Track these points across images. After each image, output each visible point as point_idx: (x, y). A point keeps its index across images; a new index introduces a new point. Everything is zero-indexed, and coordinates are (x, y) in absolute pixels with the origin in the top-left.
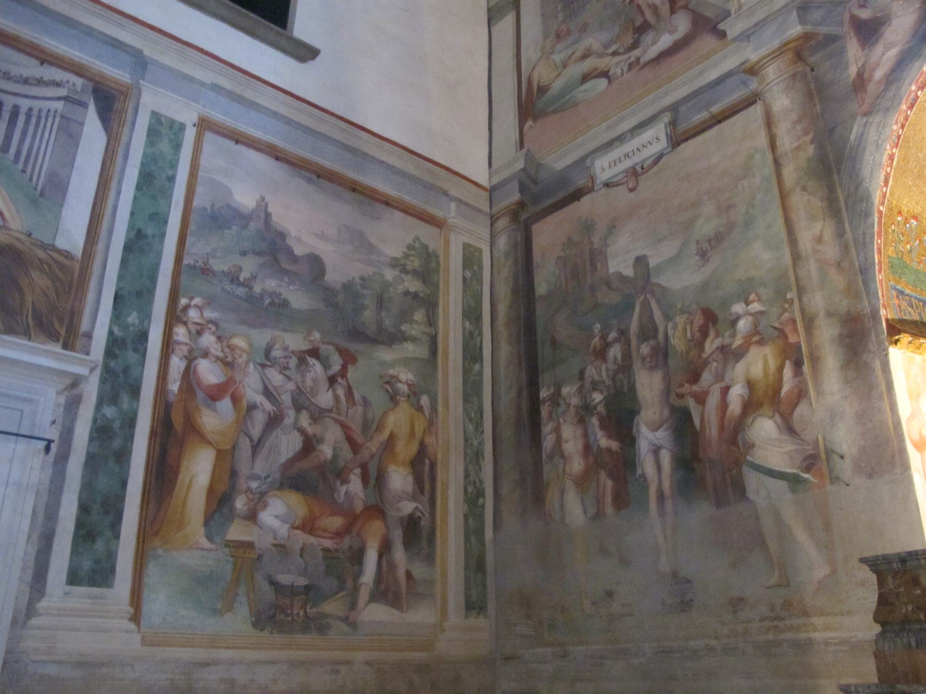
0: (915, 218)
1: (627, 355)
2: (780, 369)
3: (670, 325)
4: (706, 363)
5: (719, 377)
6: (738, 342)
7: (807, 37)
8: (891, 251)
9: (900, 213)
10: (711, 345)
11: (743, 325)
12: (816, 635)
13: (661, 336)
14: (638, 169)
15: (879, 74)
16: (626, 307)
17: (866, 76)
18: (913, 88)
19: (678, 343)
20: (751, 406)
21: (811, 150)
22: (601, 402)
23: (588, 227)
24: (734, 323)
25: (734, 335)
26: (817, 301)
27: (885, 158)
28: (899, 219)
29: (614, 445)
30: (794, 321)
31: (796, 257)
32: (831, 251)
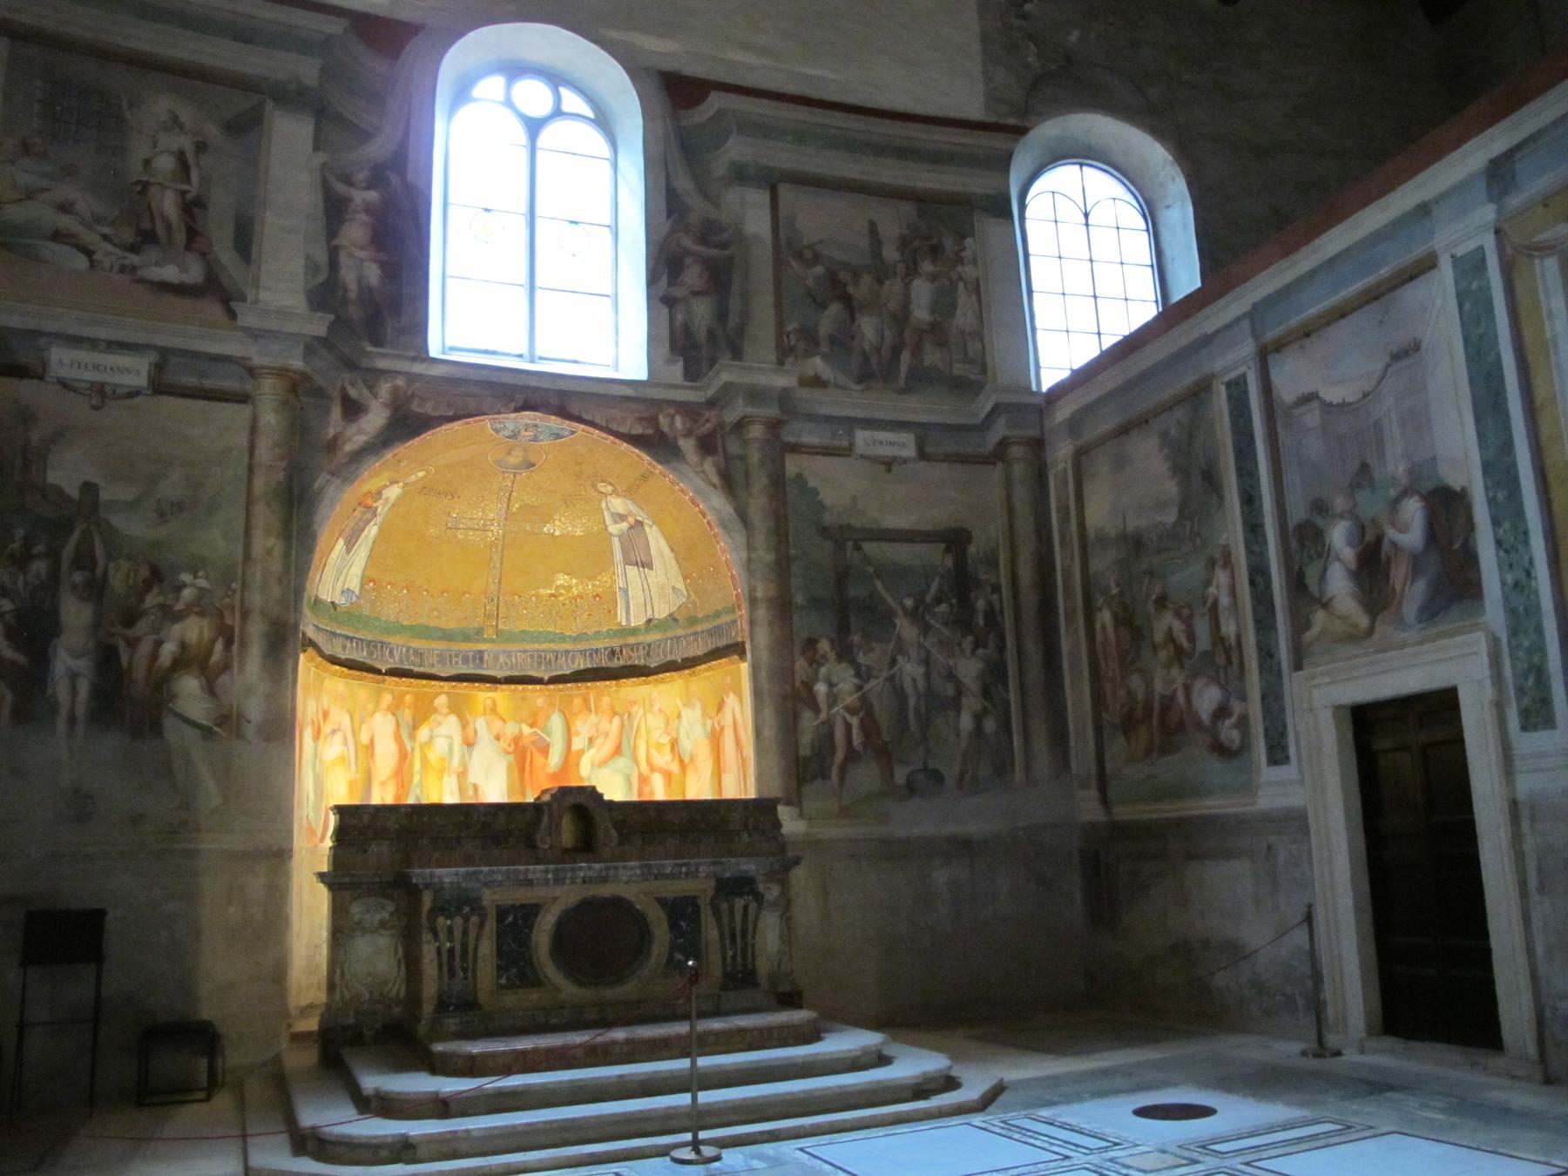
1: (54, 576)
2: (213, 642)
3: (112, 565)
4: (144, 613)
5: (156, 630)
6: (179, 607)
7: (305, 377)
10: (151, 600)
11: (187, 593)
12: (201, 846)
13: (99, 571)
14: (108, 389)
15: (349, 448)
16: (61, 528)
17: (339, 442)
19: (117, 582)
20: (182, 662)
21: (281, 476)
22: (11, 611)
23: (27, 417)
24: (179, 588)
25: (177, 599)
26: (256, 599)
29: (21, 659)
30: (233, 609)
31: (247, 556)
32: (276, 566)
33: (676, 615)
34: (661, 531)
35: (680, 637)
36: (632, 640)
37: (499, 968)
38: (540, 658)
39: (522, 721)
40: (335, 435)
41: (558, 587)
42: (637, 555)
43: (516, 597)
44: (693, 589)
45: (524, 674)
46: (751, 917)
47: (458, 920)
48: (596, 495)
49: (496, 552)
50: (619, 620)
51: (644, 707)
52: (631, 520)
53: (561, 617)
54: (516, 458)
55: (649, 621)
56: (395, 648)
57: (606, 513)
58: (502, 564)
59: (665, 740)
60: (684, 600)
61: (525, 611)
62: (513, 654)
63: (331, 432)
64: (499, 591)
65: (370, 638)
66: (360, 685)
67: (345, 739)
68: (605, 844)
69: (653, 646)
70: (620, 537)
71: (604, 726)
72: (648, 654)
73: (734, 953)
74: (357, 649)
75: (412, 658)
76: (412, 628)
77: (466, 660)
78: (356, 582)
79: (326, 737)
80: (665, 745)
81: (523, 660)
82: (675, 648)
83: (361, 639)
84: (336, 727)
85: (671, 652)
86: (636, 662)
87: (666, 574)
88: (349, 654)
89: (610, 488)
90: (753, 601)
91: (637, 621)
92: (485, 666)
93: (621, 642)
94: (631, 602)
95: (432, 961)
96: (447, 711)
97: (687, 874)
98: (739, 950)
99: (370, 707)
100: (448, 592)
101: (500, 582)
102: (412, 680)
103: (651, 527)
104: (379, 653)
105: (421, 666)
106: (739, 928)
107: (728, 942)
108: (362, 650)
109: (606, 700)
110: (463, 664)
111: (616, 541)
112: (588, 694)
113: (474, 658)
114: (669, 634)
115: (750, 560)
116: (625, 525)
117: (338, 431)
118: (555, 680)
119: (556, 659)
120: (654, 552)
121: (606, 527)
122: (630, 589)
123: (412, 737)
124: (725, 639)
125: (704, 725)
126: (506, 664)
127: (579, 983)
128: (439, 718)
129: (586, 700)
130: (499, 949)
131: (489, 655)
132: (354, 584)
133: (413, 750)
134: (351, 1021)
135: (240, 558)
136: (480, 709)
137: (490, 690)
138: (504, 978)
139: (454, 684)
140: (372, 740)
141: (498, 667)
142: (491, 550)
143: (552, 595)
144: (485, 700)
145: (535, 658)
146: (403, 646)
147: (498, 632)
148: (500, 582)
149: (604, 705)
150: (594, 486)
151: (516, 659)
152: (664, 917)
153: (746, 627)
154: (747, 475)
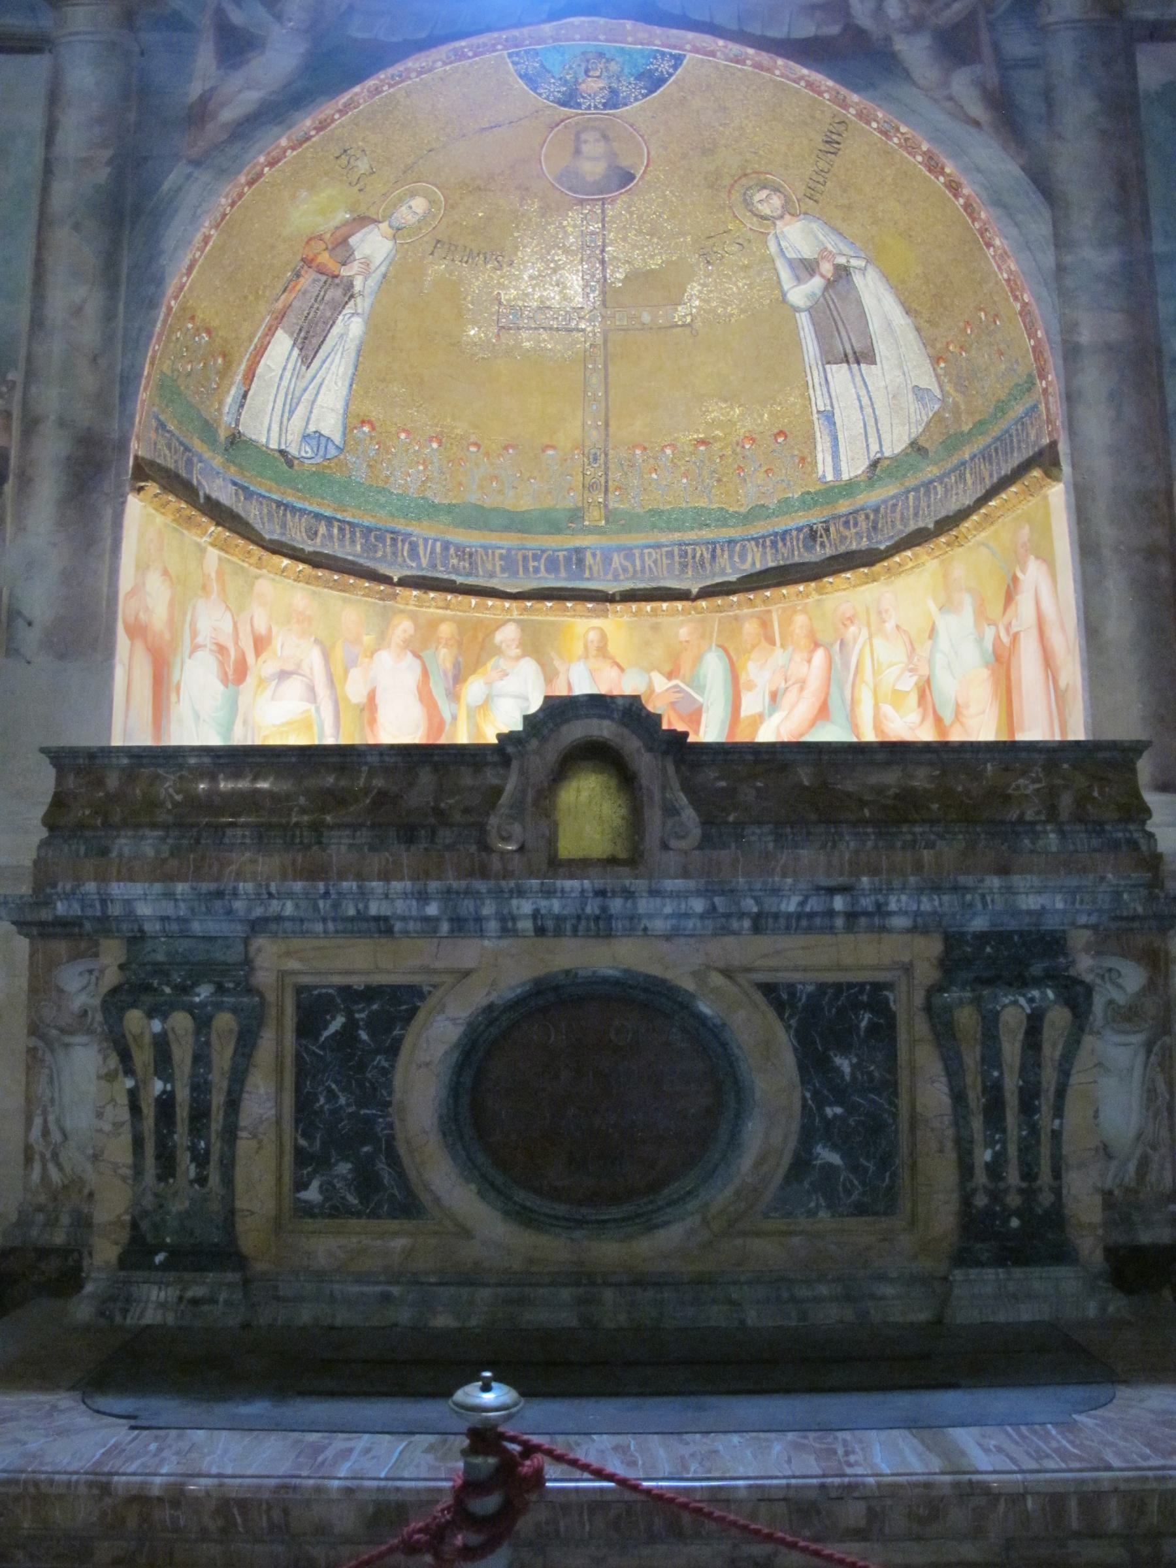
0: (208, 332)
8: (166, 367)
9: (192, 318)
15: (228, 115)
17: (211, 106)
18: (262, 159)
21: (102, 175)
27: (199, 237)
28: (190, 326)
31: (37, 323)
32: (89, 335)
33: (922, 442)
34: (886, 277)
35: (931, 482)
36: (844, 507)
37: (302, 1157)
38: (684, 556)
39: (652, 668)
40: (201, 96)
41: (712, 425)
42: (845, 339)
43: (638, 452)
44: (950, 381)
45: (654, 585)
46: (1052, 1051)
47: (181, 1021)
48: (752, 223)
49: (595, 370)
50: (820, 473)
51: (869, 625)
52: (827, 268)
53: (719, 480)
54: (593, 168)
55: (875, 464)
56: (421, 542)
57: (781, 265)
58: (606, 392)
59: (909, 683)
60: (937, 407)
61: (654, 476)
62: (637, 552)
63: (195, 90)
64: (606, 440)
65: (367, 521)
66: (344, 600)
67: (312, 689)
68: (665, 846)
69: (882, 510)
70: (809, 310)
71: (799, 668)
72: (875, 528)
73: (996, 1156)
74: (342, 540)
75: (455, 561)
76: (450, 509)
77: (553, 566)
78: (333, 421)
79: (262, 682)
80: (908, 692)
81: (655, 562)
82: (923, 504)
83: (349, 523)
84: (289, 667)
85: (916, 514)
86: (854, 547)
87: (901, 367)
88: (323, 545)
89: (777, 201)
90: (1071, 353)
91: (853, 467)
92: (587, 575)
93: (826, 513)
94: (840, 436)
95: (117, 1125)
96: (518, 651)
97: (852, 916)
98: (1012, 1150)
99: (368, 639)
100: (513, 447)
101: (607, 425)
102: (449, 597)
103: (863, 271)
104: (388, 549)
105: (469, 575)
106: (1011, 1084)
107: (977, 1123)
108: (353, 541)
109: (800, 620)
110: (548, 570)
111: (804, 319)
112: (769, 611)
113: (568, 560)
114: (911, 482)
115: (1061, 270)
116: (816, 283)
117: (207, 87)
118: (707, 593)
119: (714, 557)
120: (875, 325)
121: (784, 295)
122: (837, 411)
123: (454, 695)
124: (1015, 454)
125: (980, 639)
126: (625, 570)
127: (525, 1217)
128: (503, 663)
129: (765, 624)
130: (304, 1106)
131: (594, 555)
132: (330, 424)
133: (454, 718)
134: (59, 1238)
135: (23, 325)
136: (579, 649)
137: (594, 614)
138: (315, 1184)
139: (529, 604)
140: (372, 697)
141: (610, 577)
142: (585, 367)
143: (703, 442)
144: (587, 632)
145: (677, 558)
146: (436, 540)
147: (610, 515)
148: (607, 425)
149: (797, 631)
150: (748, 204)
151: (643, 561)
152: (784, 1042)
153: (1056, 407)
154: (1047, 95)
